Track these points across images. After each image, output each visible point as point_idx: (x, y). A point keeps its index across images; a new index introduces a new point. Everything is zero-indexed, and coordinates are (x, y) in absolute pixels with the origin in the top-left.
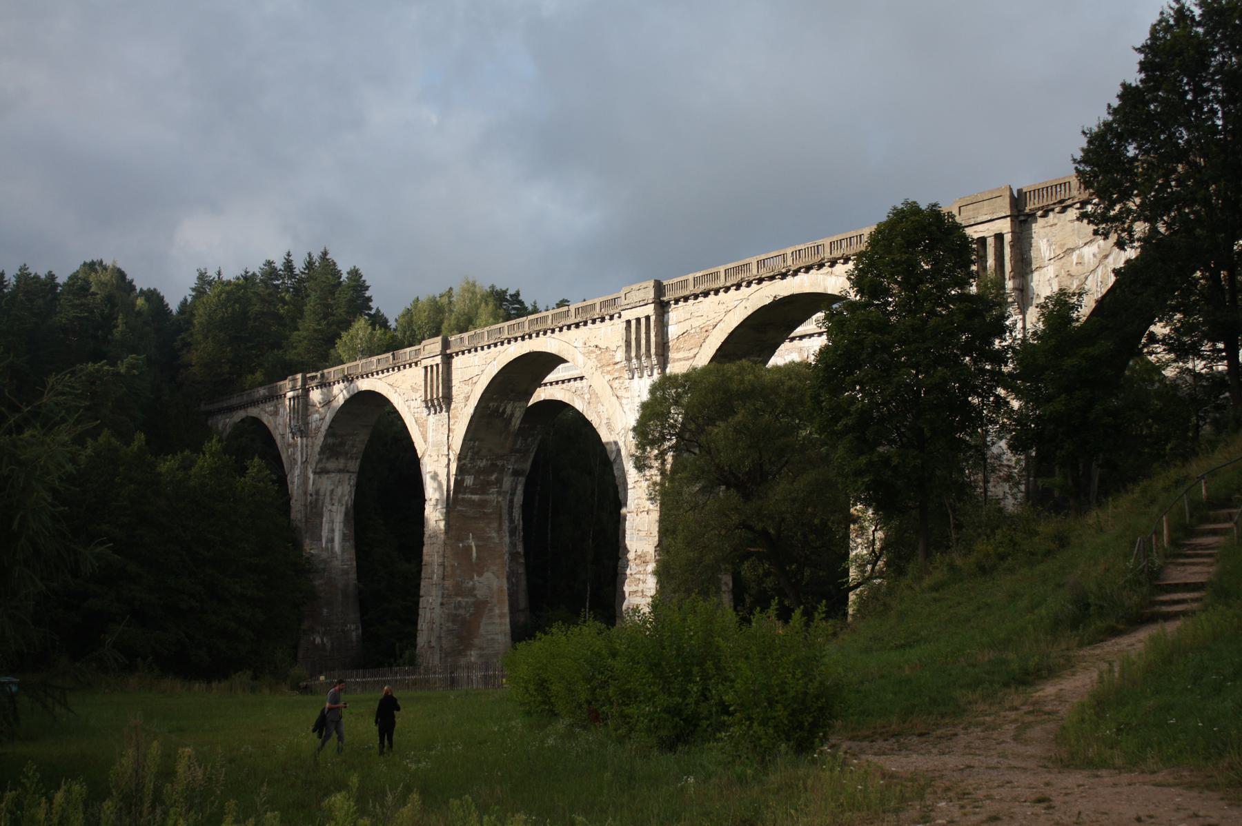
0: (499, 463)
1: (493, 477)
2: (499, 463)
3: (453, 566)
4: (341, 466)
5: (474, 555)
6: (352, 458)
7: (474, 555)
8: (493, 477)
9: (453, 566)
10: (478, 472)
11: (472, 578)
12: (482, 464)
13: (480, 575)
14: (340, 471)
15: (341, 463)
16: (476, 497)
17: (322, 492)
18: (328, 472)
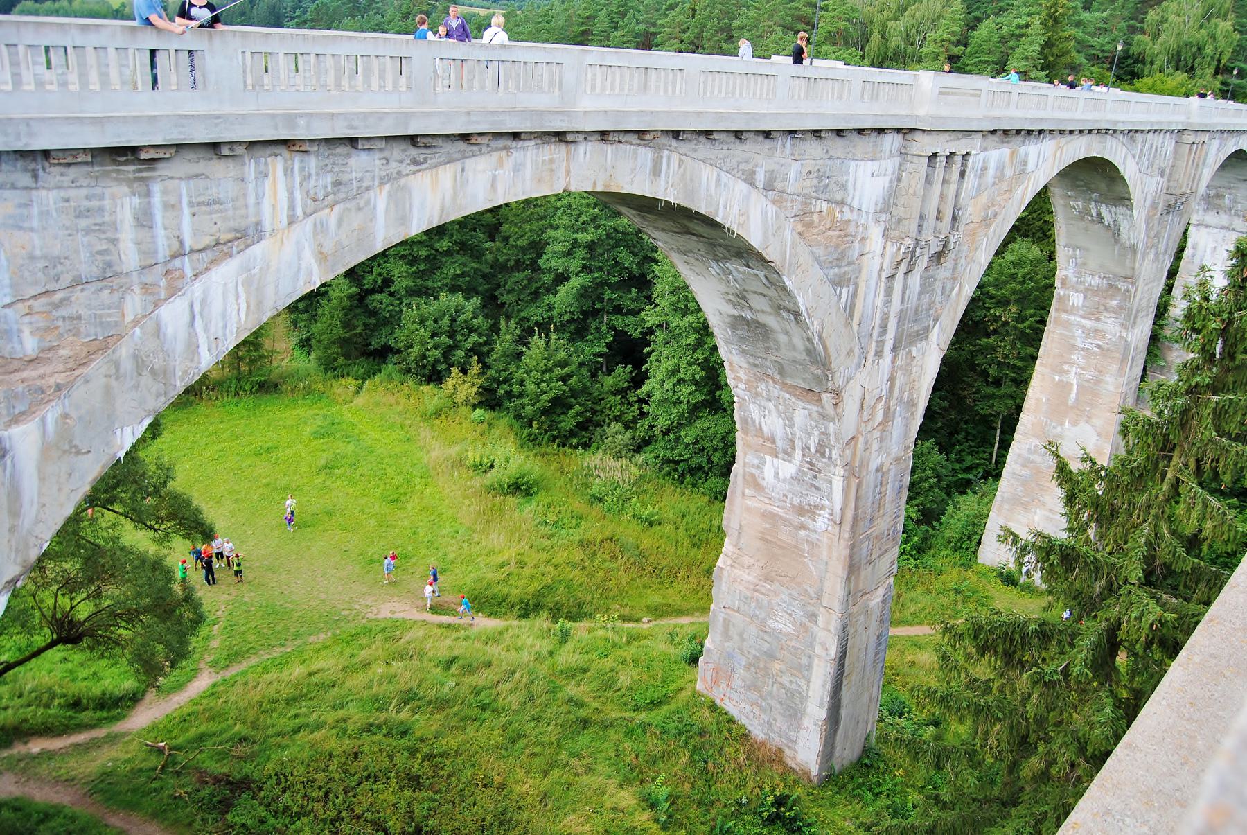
0: (1122, 286)
1: (1114, 303)
2: (1122, 286)
3: (1038, 399)
4: (1225, 223)
5: (1073, 396)
6: (1236, 214)
7: (1073, 396)
8: (1114, 303)
9: (1038, 399)
10: (1088, 291)
11: (1062, 424)
12: (1095, 281)
13: (1075, 424)
14: (1223, 228)
15: (1224, 219)
16: (1088, 323)
17: (1200, 247)
18: (1207, 226)
